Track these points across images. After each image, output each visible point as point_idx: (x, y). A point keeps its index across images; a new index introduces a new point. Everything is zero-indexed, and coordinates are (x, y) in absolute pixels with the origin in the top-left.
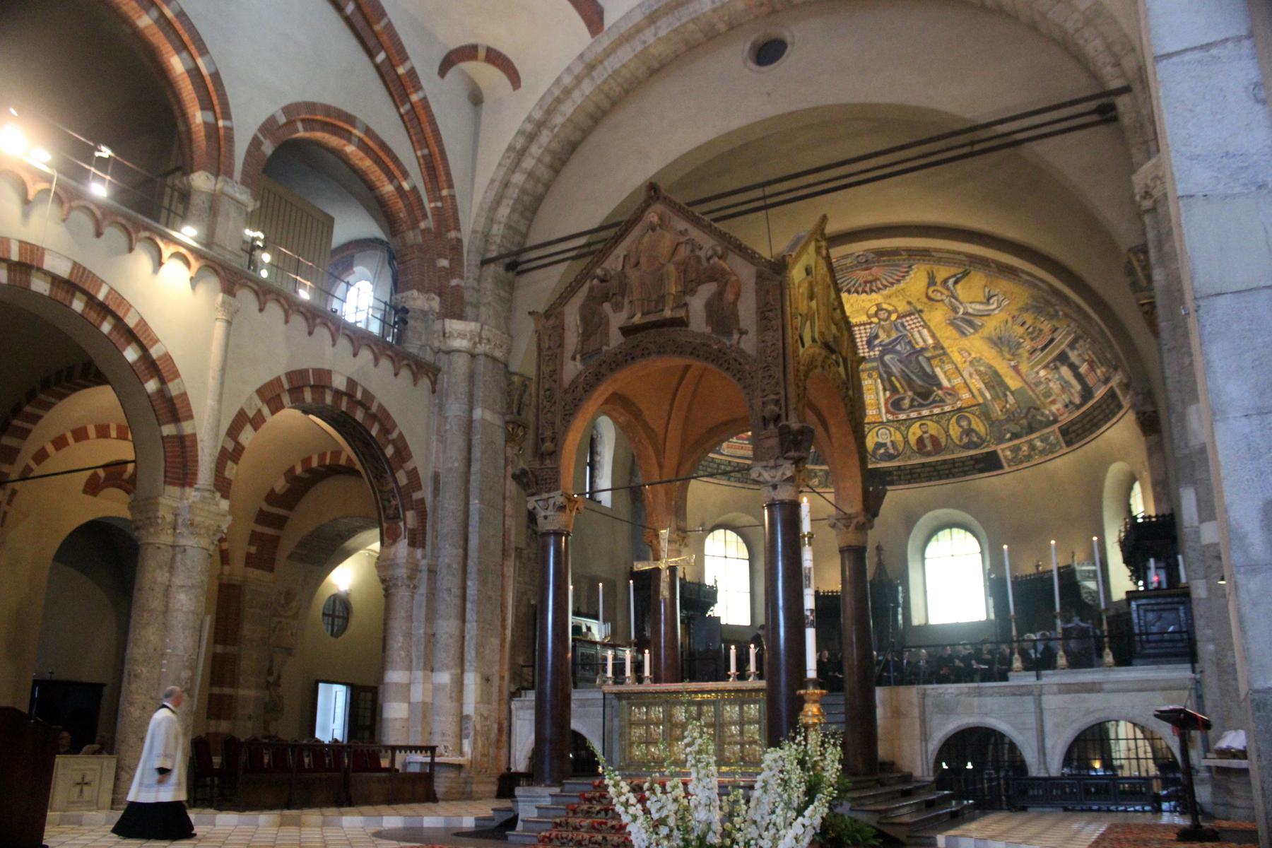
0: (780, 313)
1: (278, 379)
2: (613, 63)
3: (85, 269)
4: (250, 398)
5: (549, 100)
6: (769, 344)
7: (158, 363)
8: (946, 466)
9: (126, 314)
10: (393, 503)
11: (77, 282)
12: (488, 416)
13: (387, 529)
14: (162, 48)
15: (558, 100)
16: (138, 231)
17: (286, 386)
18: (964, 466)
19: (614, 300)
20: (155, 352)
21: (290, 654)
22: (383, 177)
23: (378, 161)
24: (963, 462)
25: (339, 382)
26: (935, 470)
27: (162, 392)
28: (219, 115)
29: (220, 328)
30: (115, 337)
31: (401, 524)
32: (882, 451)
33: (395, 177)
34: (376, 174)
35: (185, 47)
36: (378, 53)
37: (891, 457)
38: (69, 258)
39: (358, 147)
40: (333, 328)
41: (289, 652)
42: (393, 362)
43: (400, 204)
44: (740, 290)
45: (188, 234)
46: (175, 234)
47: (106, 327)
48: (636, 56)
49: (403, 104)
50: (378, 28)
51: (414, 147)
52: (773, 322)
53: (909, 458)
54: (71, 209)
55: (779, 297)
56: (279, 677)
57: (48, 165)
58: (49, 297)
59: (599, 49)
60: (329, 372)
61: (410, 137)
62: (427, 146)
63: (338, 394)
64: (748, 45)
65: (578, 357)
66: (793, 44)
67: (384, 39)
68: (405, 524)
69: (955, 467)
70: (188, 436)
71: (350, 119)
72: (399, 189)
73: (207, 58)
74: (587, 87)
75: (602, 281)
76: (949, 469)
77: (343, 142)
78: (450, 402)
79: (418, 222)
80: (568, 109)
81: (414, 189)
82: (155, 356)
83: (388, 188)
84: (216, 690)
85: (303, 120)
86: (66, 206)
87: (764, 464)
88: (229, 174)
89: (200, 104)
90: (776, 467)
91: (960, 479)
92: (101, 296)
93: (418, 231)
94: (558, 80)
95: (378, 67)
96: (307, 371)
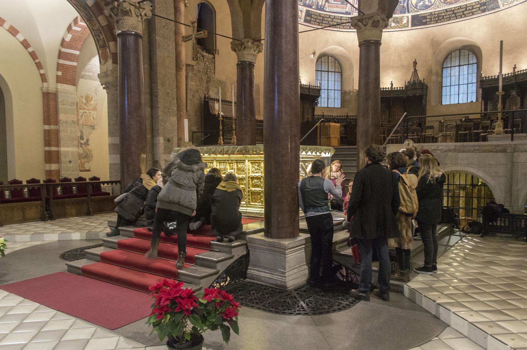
8: (461, 10)
10: (101, 37)
13: (102, 53)
18: (473, 9)
21: (94, 129)
24: (472, 6)
26: (453, 13)
31: (108, 50)
32: (421, 3)
37: (427, 7)
41: (93, 127)
53: (438, 7)
56: (88, 140)
68: (109, 50)
69: (466, 10)
76: (463, 12)
84: (47, 149)
91: (469, 18)
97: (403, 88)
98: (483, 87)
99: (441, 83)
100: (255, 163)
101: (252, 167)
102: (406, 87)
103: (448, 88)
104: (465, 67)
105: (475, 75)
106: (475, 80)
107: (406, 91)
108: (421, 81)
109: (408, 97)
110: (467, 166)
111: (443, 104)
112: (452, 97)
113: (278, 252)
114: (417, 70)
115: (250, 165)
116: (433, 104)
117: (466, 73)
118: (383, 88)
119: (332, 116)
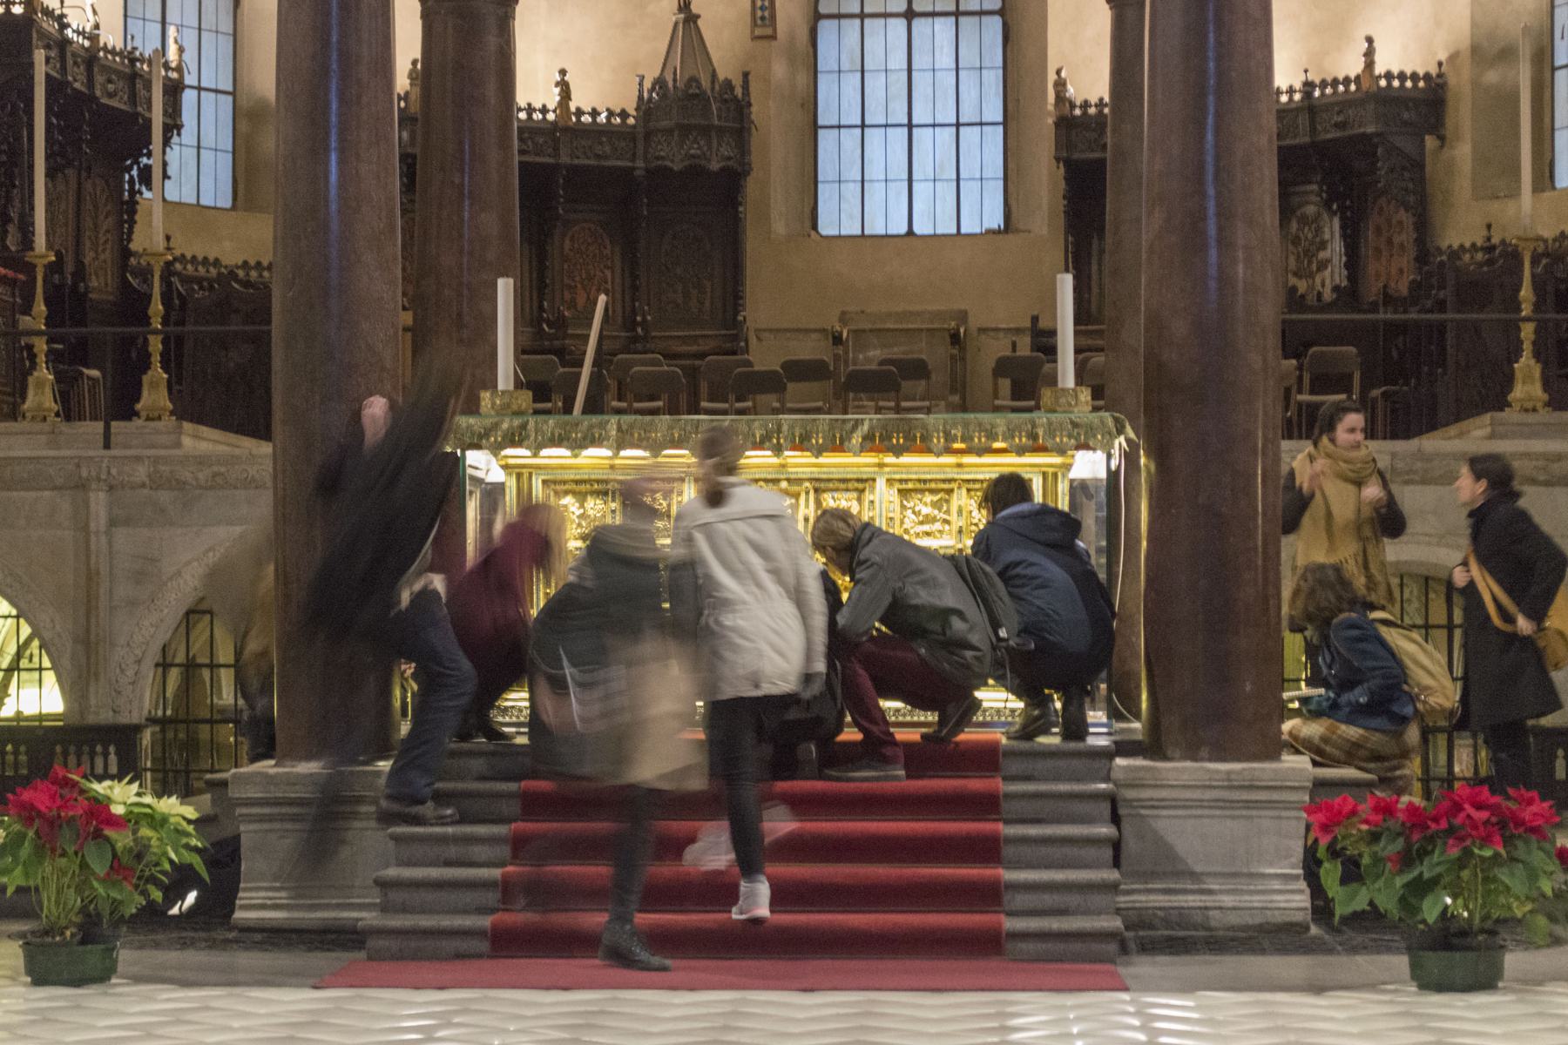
97: (624, 114)
98: (1076, 156)
99: (811, 102)
100: (922, 491)
101: (903, 507)
102: (646, 108)
103: (851, 138)
104: (944, 27)
105: (994, 79)
106: (994, 111)
107: (648, 135)
108: (728, 84)
109: (659, 175)
110: (1438, 544)
111: (827, 227)
112: (875, 193)
113: (1270, 805)
114: (698, 16)
115: (896, 498)
116: (779, 227)
117: (946, 59)
118: (530, 109)
119: (217, 262)
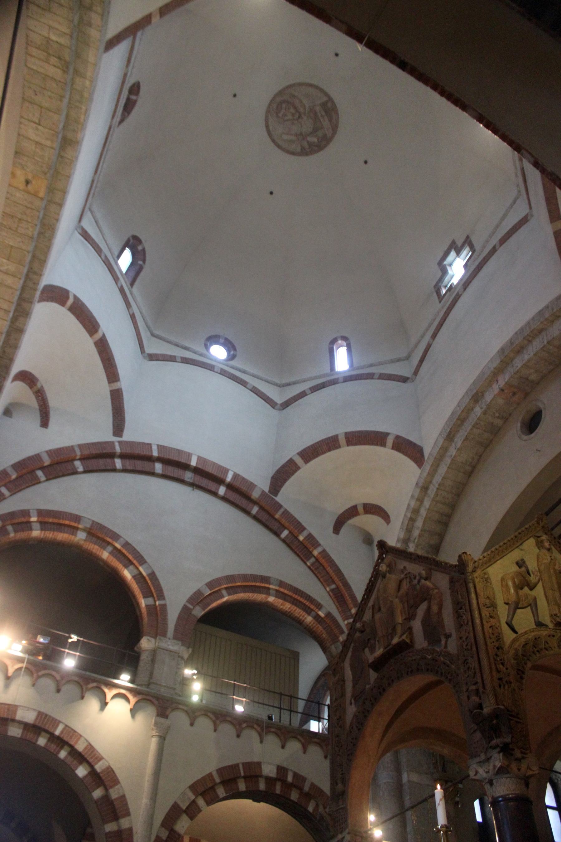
0: (468, 607)
1: (210, 775)
2: (437, 479)
3: (46, 715)
4: (184, 793)
5: (406, 522)
6: (464, 639)
7: (101, 775)
9: (76, 742)
11: (40, 725)
12: (415, 777)
14: (118, 567)
15: (412, 520)
16: (87, 683)
17: (218, 780)
19: (369, 645)
20: (99, 767)
22: (303, 613)
23: (295, 602)
25: (269, 770)
27: (106, 798)
28: (156, 599)
29: (154, 741)
30: (69, 760)
33: (312, 610)
34: (298, 612)
35: (131, 563)
36: (281, 533)
38: (34, 710)
39: (276, 596)
40: (259, 729)
42: (321, 747)
43: (320, 628)
44: (441, 600)
45: (124, 679)
46: (116, 681)
47: (63, 754)
48: (448, 467)
49: (308, 560)
50: (277, 516)
51: (324, 586)
52: (464, 617)
54: (39, 677)
55: (465, 594)
57: (22, 652)
58: (21, 739)
59: (425, 474)
60: (259, 764)
61: (319, 580)
62: (334, 582)
63: (269, 780)
64: (519, 425)
65: (353, 701)
66: (545, 409)
67: (283, 521)
70: (125, 830)
71: (265, 579)
72: (317, 618)
73: (145, 566)
74: (427, 503)
75: (362, 632)
77: (264, 596)
78: (380, 772)
79: (338, 638)
80: (419, 523)
81: (329, 615)
82: (99, 770)
83: (309, 619)
85: (226, 588)
86: (35, 675)
87: (477, 760)
88: (164, 634)
89: (143, 595)
90: (488, 760)
92: (57, 732)
93: (339, 644)
94: (409, 505)
95: (284, 541)
96: (237, 765)
